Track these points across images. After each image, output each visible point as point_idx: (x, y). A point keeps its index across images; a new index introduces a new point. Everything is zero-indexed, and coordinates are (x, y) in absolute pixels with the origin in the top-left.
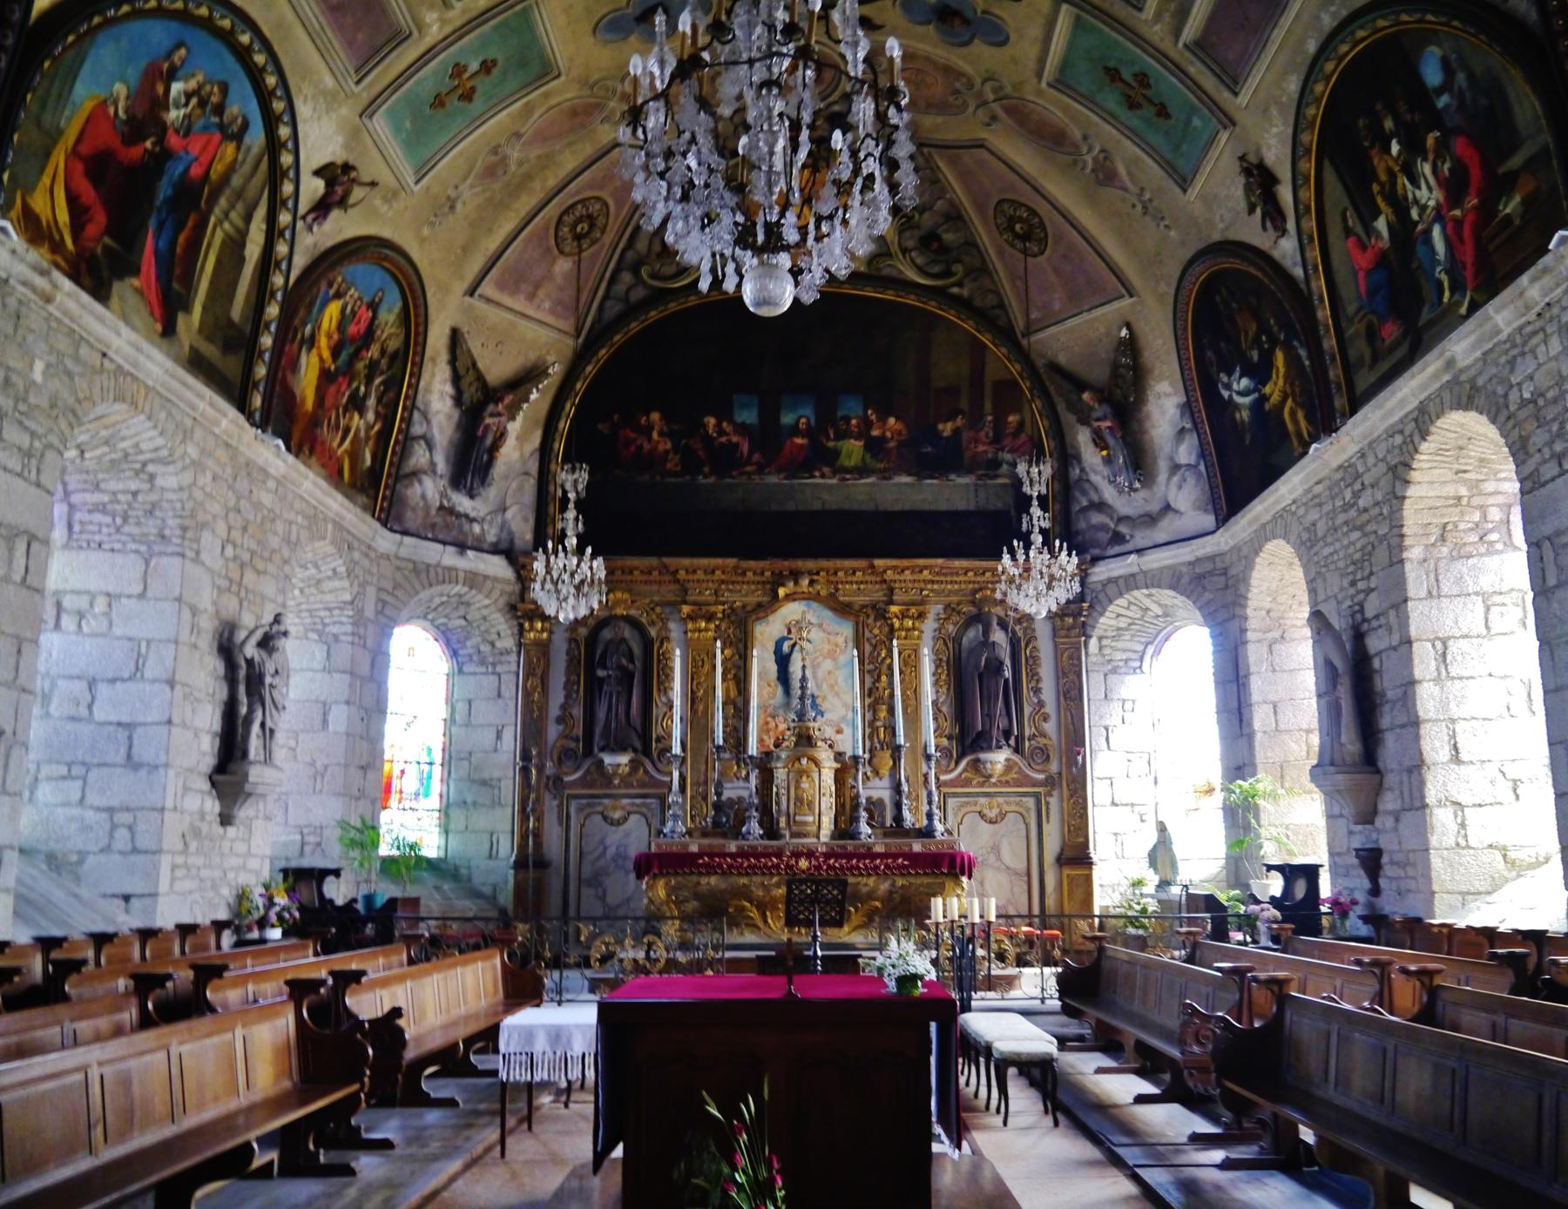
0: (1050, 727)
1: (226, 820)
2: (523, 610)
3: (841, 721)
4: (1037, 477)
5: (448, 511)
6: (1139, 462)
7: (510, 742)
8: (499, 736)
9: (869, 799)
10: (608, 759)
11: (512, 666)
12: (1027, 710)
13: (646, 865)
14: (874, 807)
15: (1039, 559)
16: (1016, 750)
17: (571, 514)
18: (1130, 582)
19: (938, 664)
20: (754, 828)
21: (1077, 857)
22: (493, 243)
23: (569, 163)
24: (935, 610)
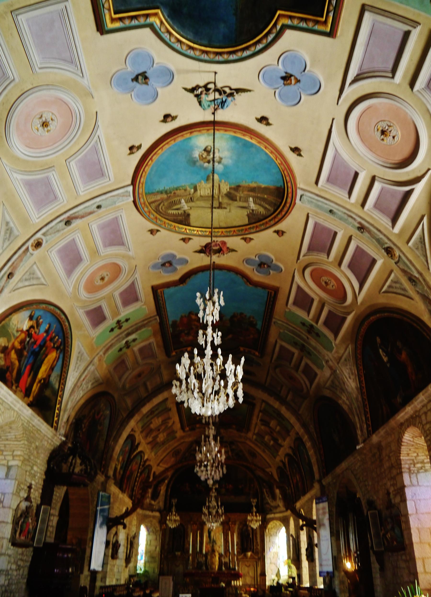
0: (259, 547)
1: (126, 566)
2: (162, 521)
3: (220, 548)
4: (254, 502)
5: (151, 504)
6: (274, 497)
7: (158, 549)
8: (156, 548)
9: (225, 562)
10: (177, 553)
11: (160, 534)
12: (255, 544)
13: (186, 575)
14: (226, 563)
15: (255, 518)
16: (253, 552)
17: (174, 508)
18: (273, 519)
19: (238, 534)
20: (204, 568)
21: (263, 574)
22: (162, 457)
23: (176, 444)
24: (238, 523)
